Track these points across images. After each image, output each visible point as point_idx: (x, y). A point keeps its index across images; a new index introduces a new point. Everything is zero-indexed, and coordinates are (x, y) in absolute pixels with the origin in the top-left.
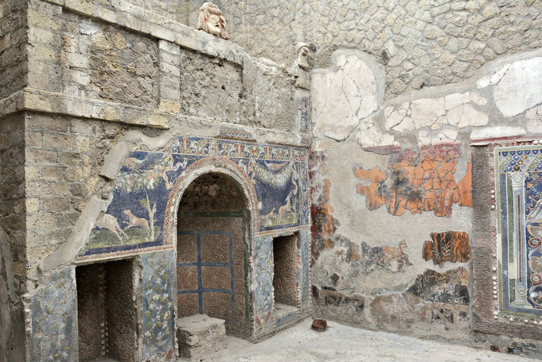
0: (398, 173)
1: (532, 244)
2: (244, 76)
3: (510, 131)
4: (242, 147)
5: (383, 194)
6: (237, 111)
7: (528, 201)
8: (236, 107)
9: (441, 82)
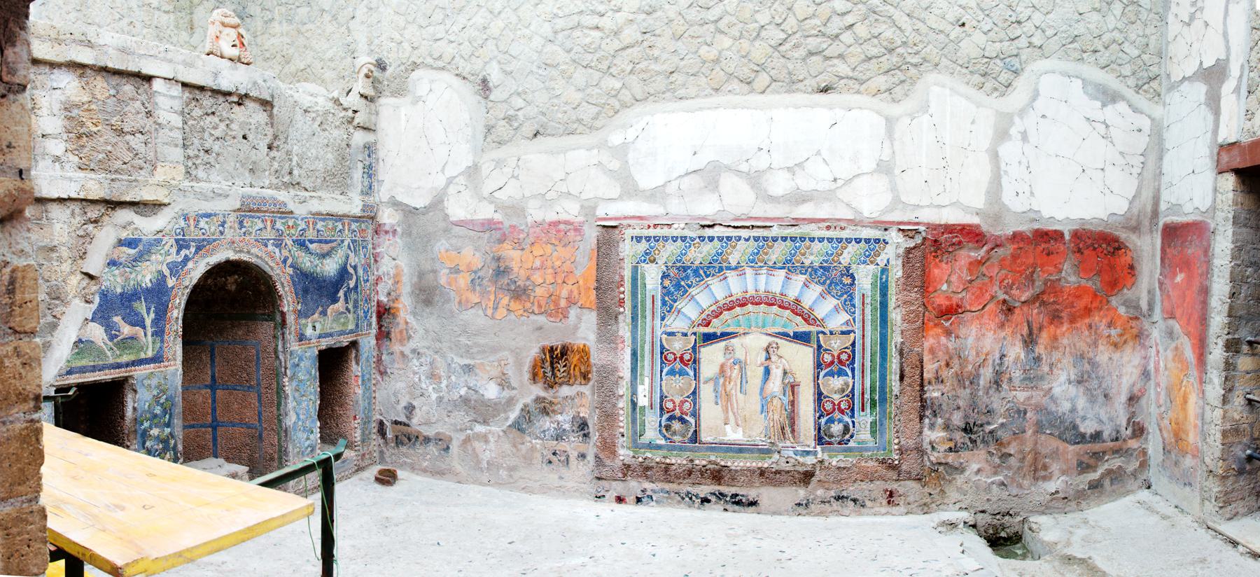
0: (499, 259)
1: (666, 360)
2: (275, 118)
3: (645, 209)
4: (273, 223)
5: (478, 288)
6: (265, 170)
7: (664, 303)
8: (265, 163)
9: (561, 132)
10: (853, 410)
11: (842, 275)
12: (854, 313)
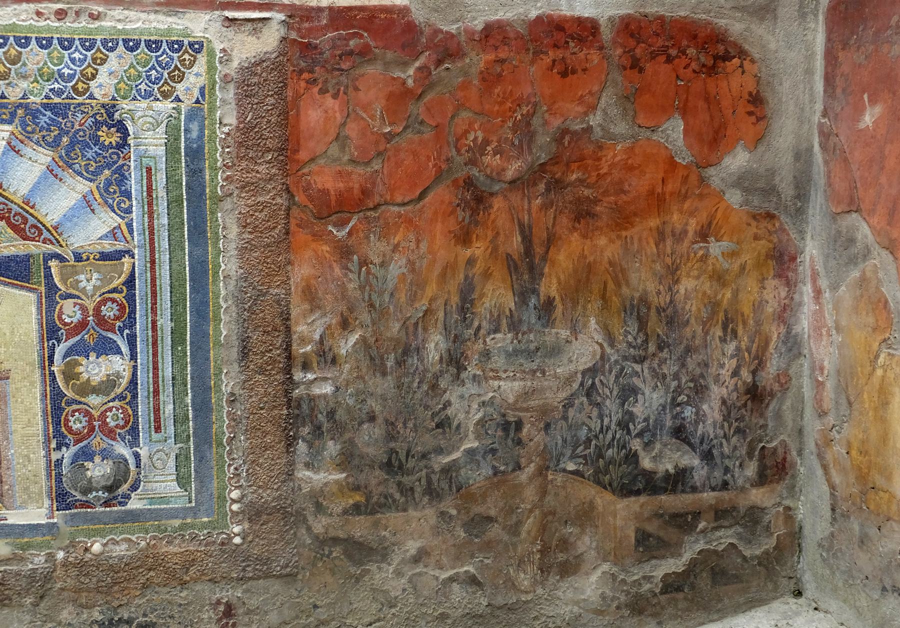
10: (134, 431)
11: (98, 125)
12: (129, 211)
